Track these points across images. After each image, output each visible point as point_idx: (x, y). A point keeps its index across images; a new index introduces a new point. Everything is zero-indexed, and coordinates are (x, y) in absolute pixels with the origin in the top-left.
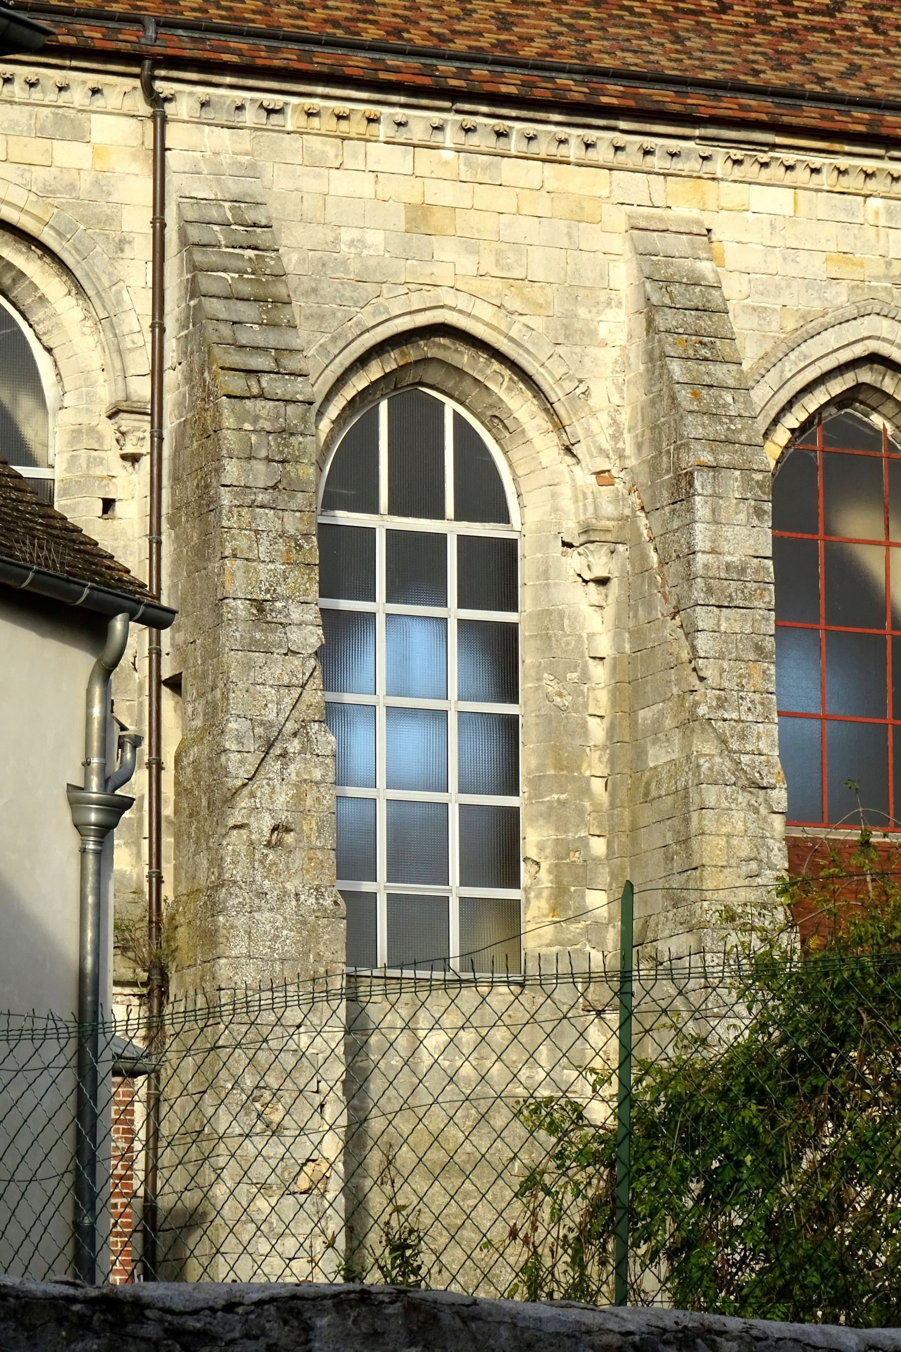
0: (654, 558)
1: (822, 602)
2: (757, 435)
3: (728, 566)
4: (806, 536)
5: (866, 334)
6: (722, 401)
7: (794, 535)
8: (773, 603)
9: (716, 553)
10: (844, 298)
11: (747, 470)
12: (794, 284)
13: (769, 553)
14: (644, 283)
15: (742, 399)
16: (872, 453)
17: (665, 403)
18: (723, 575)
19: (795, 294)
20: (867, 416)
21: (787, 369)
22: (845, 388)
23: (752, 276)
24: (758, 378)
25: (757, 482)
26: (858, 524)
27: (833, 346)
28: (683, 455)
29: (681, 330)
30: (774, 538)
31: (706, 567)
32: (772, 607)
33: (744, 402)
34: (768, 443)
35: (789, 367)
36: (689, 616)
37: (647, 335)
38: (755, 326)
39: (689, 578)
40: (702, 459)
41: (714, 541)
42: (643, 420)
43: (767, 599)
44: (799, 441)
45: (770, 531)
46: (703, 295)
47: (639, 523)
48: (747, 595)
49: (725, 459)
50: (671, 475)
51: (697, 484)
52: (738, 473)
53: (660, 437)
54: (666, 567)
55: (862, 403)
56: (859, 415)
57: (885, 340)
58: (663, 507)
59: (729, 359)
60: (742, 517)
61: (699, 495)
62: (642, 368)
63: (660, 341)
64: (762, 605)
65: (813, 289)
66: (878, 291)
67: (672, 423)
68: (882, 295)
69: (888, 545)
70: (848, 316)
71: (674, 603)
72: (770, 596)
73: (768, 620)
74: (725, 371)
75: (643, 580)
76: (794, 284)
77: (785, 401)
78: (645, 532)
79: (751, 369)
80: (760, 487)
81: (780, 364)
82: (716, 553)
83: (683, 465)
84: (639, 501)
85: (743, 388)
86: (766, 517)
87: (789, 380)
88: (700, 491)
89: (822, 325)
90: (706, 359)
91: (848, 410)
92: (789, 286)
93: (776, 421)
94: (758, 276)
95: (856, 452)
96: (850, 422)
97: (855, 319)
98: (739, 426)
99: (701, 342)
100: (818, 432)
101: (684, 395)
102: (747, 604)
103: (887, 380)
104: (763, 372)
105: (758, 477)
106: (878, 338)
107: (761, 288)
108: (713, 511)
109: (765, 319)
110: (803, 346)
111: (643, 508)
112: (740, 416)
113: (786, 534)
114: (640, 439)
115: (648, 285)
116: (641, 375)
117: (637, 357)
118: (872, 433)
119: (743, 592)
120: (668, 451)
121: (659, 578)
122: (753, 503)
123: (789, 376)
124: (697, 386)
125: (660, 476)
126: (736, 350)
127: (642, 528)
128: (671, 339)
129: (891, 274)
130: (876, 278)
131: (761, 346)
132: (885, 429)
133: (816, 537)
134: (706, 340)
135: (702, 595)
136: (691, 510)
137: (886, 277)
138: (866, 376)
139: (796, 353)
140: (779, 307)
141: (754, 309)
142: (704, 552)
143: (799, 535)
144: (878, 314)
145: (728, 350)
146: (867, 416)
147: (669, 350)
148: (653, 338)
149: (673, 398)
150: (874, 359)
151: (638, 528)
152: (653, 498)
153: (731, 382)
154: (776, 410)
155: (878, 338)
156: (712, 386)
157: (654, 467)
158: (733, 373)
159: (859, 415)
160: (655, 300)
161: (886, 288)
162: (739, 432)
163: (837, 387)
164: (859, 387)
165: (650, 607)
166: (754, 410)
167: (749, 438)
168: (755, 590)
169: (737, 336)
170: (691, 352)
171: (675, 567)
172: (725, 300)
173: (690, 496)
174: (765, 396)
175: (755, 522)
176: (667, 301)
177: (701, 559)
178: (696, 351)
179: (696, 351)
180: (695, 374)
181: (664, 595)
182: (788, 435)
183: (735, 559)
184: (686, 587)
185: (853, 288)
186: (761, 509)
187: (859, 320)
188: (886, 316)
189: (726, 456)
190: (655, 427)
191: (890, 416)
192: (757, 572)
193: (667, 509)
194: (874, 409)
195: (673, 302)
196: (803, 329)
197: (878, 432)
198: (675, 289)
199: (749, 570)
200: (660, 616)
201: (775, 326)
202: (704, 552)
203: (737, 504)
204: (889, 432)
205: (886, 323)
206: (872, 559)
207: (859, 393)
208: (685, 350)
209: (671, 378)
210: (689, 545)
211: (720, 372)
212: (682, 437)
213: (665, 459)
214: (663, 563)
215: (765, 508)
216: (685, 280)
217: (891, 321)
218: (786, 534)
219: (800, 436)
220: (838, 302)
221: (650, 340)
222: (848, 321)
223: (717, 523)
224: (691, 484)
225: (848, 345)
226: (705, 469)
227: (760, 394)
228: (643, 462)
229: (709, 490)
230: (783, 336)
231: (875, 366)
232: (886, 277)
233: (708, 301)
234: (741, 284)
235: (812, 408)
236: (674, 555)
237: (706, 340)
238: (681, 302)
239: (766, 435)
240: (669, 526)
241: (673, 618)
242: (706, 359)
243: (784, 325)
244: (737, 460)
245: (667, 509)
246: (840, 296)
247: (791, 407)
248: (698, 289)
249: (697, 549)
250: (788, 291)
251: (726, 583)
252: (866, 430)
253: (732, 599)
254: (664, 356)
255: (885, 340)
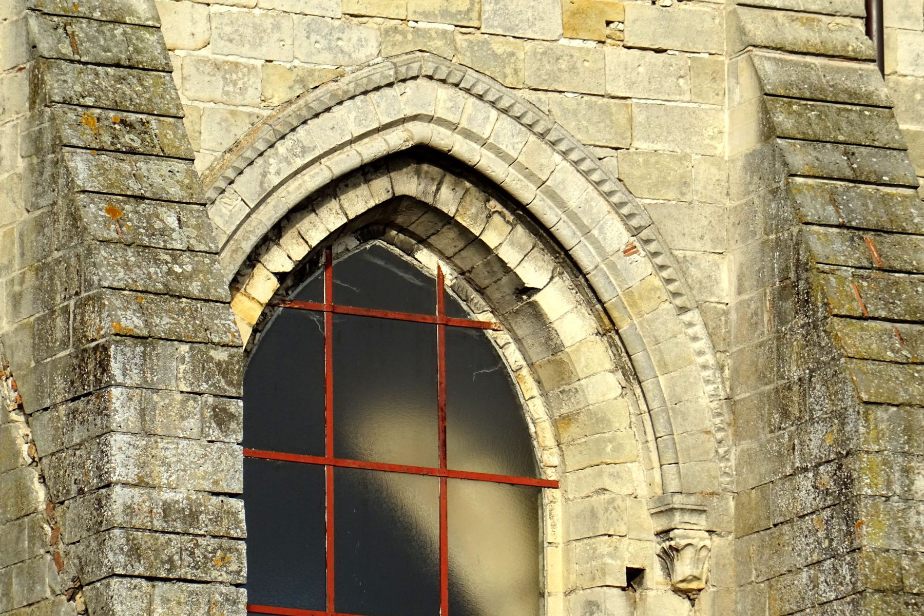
0: (40, 493)
1: (330, 572)
2: (219, 283)
3: (167, 509)
4: (303, 458)
5: (409, 112)
6: (158, 225)
7: (283, 456)
8: (244, 573)
9: (147, 486)
10: (371, 49)
11: (201, 343)
12: (286, 23)
13: (238, 487)
14: (26, 18)
15: (193, 221)
16: (418, 317)
17: (60, 226)
18: (158, 524)
19: (288, 41)
20: (410, 253)
21: (272, 170)
22: (372, 204)
23: (214, 9)
24: (222, 184)
25: (219, 364)
26: (395, 439)
27: (351, 132)
28: (92, 318)
29: (89, 101)
30: (247, 462)
31: (129, 510)
32: (242, 580)
33: (198, 227)
34: (239, 297)
35: (276, 166)
36: (99, 595)
37: (31, 108)
38: (218, 95)
39: (100, 529)
40: (124, 323)
41: (142, 466)
42: (22, 254)
43: (234, 567)
44: (292, 295)
45: (239, 449)
46: (129, 41)
47: (14, 433)
48: (200, 559)
49: (163, 323)
50: (70, 350)
51: (115, 368)
52: (184, 348)
53: (52, 284)
54: (60, 509)
55: (401, 230)
56: (397, 251)
57: (441, 122)
58: (55, 406)
59: (172, 152)
60: (192, 424)
61: (118, 385)
62: (21, 165)
63: (53, 119)
64: (225, 577)
65: (318, 32)
66: (431, 38)
67: (73, 261)
68: (437, 44)
69: (445, 475)
70: (377, 80)
71: (73, 572)
72: (239, 562)
73: (235, 603)
74: (165, 172)
75: (21, 531)
76: (286, 23)
77: (269, 224)
78: (25, 448)
79: (211, 168)
80: (224, 374)
81: (260, 161)
82: (147, 486)
83: (91, 334)
84: (14, 395)
85: (196, 203)
86: (233, 425)
87: (276, 188)
88: (119, 379)
89: (333, 95)
90: (132, 152)
91: (378, 242)
92: (277, 27)
93: (253, 260)
94: (224, 9)
95: (391, 315)
96: (381, 263)
97: (390, 85)
98: (189, 268)
99: (123, 122)
100: (326, 278)
101: (93, 213)
102: (200, 575)
103: (445, 192)
104: (231, 174)
105: (221, 355)
106: (430, 119)
107: (228, 29)
108: (142, 413)
109: (235, 84)
110: (301, 131)
111: (20, 407)
112: (189, 250)
113: (270, 455)
114: (17, 288)
115: (33, 22)
116: (20, 177)
117: (13, 145)
118: (418, 283)
119: (192, 554)
120: (66, 310)
121: (47, 527)
122: (211, 400)
123: (276, 182)
124: (117, 198)
125: (51, 352)
126: (184, 136)
127: (20, 441)
128: (71, 116)
129: (453, 9)
130: (428, 16)
131: (228, 131)
132: (441, 276)
133: (320, 460)
134: (132, 117)
135: (122, 558)
136: (103, 412)
137: (445, 14)
138: (408, 184)
139: (288, 142)
140: (259, 63)
141: (217, 66)
142: (125, 484)
143: (292, 457)
144: (430, 78)
145: (170, 135)
146: (410, 253)
147: (68, 134)
148: (41, 113)
149: (75, 217)
150: (422, 155)
151: (13, 442)
152: (39, 388)
153: (175, 192)
154: (254, 240)
155: (430, 119)
156: (143, 198)
157: (41, 336)
158: (179, 177)
159: (397, 251)
160: (44, 47)
161: (445, 32)
162: (189, 277)
163: (359, 202)
164: (397, 202)
165: (33, 578)
166: (214, 240)
167: (205, 287)
168: (214, 551)
169: (186, 111)
170: (107, 139)
171: (75, 510)
172: (166, 50)
173: (102, 387)
174: (232, 216)
175: (215, 433)
176: (66, 50)
177: (120, 496)
178: (115, 137)
179: (115, 137)
180: (112, 177)
181: (56, 559)
182: (274, 283)
183: (179, 497)
184: (94, 544)
185: (387, 31)
186: (224, 410)
187: (398, 89)
188: (444, 81)
189: (166, 320)
190: (42, 268)
191: (450, 252)
192: (217, 520)
193: (62, 409)
194: (423, 242)
195: (76, 51)
196: (301, 102)
197: (429, 280)
198: (80, 29)
199: (202, 517)
200: (48, 594)
201: (252, 95)
202: (125, 484)
203: (184, 403)
204: (448, 282)
205: (444, 93)
206: (418, 499)
207: (396, 212)
208: (97, 135)
209: (70, 183)
210: (101, 473)
211: (157, 174)
212: (90, 285)
213: (59, 322)
214: (54, 502)
215: (232, 409)
216: (97, 14)
217: (452, 91)
218: (270, 455)
219: (295, 286)
220: (361, 56)
221: (35, 117)
222: (378, 89)
223: (148, 435)
224: (104, 366)
225: (378, 130)
226: (129, 342)
227: (225, 213)
228: (23, 327)
229: (135, 378)
230: (266, 113)
231: (425, 167)
232: (445, 14)
233: (138, 51)
234: (194, 22)
235: (316, 236)
236: (74, 489)
237: (132, 117)
238: (90, 52)
239: (236, 284)
240: (66, 439)
241: (72, 598)
242: (132, 152)
243: (268, 94)
244: (184, 325)
245: (62, 409)
246: (364, 46)
247: (279, 236)
248: (119, 31)
249: (114, 479)
250: (276, 36)
251: (163, 538)
252: (407, 277)
253: (173, 567)
254: (59, 144)
255: (441, 122)
